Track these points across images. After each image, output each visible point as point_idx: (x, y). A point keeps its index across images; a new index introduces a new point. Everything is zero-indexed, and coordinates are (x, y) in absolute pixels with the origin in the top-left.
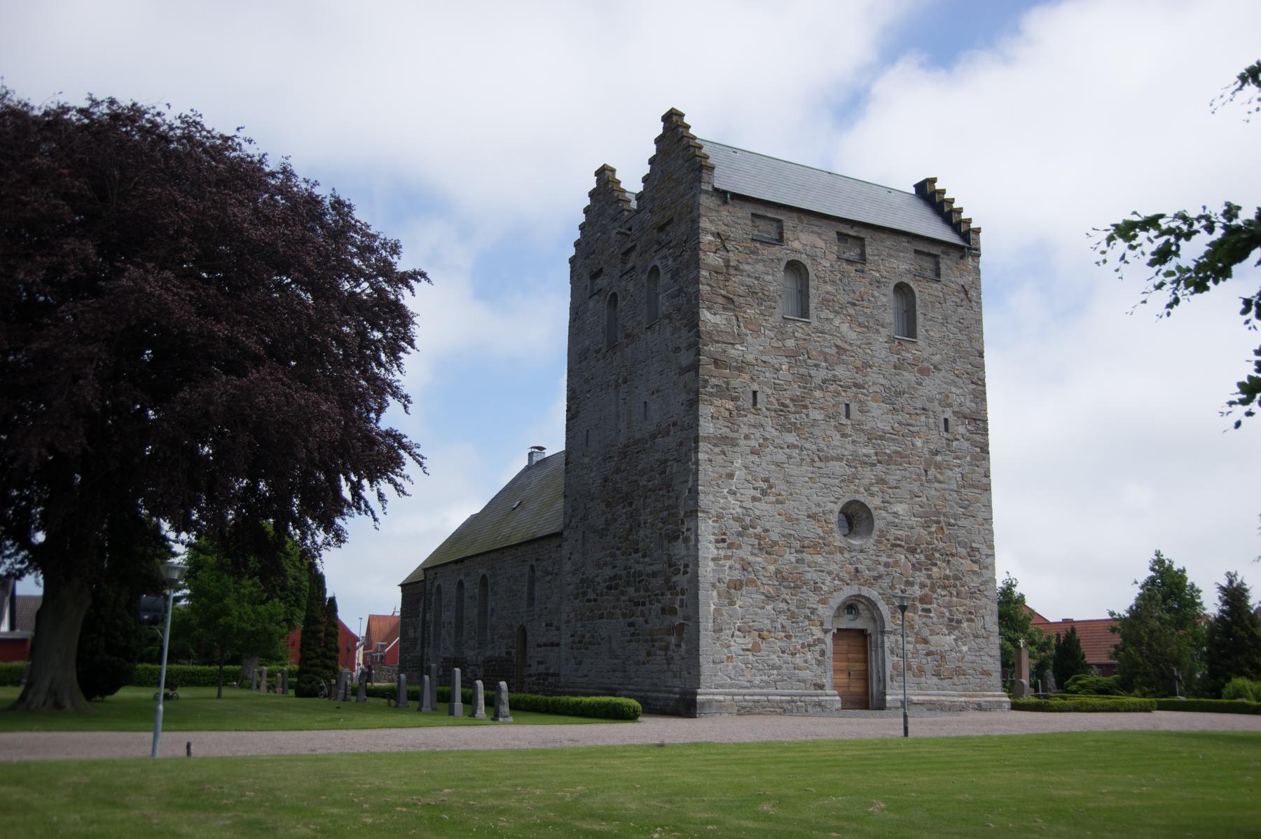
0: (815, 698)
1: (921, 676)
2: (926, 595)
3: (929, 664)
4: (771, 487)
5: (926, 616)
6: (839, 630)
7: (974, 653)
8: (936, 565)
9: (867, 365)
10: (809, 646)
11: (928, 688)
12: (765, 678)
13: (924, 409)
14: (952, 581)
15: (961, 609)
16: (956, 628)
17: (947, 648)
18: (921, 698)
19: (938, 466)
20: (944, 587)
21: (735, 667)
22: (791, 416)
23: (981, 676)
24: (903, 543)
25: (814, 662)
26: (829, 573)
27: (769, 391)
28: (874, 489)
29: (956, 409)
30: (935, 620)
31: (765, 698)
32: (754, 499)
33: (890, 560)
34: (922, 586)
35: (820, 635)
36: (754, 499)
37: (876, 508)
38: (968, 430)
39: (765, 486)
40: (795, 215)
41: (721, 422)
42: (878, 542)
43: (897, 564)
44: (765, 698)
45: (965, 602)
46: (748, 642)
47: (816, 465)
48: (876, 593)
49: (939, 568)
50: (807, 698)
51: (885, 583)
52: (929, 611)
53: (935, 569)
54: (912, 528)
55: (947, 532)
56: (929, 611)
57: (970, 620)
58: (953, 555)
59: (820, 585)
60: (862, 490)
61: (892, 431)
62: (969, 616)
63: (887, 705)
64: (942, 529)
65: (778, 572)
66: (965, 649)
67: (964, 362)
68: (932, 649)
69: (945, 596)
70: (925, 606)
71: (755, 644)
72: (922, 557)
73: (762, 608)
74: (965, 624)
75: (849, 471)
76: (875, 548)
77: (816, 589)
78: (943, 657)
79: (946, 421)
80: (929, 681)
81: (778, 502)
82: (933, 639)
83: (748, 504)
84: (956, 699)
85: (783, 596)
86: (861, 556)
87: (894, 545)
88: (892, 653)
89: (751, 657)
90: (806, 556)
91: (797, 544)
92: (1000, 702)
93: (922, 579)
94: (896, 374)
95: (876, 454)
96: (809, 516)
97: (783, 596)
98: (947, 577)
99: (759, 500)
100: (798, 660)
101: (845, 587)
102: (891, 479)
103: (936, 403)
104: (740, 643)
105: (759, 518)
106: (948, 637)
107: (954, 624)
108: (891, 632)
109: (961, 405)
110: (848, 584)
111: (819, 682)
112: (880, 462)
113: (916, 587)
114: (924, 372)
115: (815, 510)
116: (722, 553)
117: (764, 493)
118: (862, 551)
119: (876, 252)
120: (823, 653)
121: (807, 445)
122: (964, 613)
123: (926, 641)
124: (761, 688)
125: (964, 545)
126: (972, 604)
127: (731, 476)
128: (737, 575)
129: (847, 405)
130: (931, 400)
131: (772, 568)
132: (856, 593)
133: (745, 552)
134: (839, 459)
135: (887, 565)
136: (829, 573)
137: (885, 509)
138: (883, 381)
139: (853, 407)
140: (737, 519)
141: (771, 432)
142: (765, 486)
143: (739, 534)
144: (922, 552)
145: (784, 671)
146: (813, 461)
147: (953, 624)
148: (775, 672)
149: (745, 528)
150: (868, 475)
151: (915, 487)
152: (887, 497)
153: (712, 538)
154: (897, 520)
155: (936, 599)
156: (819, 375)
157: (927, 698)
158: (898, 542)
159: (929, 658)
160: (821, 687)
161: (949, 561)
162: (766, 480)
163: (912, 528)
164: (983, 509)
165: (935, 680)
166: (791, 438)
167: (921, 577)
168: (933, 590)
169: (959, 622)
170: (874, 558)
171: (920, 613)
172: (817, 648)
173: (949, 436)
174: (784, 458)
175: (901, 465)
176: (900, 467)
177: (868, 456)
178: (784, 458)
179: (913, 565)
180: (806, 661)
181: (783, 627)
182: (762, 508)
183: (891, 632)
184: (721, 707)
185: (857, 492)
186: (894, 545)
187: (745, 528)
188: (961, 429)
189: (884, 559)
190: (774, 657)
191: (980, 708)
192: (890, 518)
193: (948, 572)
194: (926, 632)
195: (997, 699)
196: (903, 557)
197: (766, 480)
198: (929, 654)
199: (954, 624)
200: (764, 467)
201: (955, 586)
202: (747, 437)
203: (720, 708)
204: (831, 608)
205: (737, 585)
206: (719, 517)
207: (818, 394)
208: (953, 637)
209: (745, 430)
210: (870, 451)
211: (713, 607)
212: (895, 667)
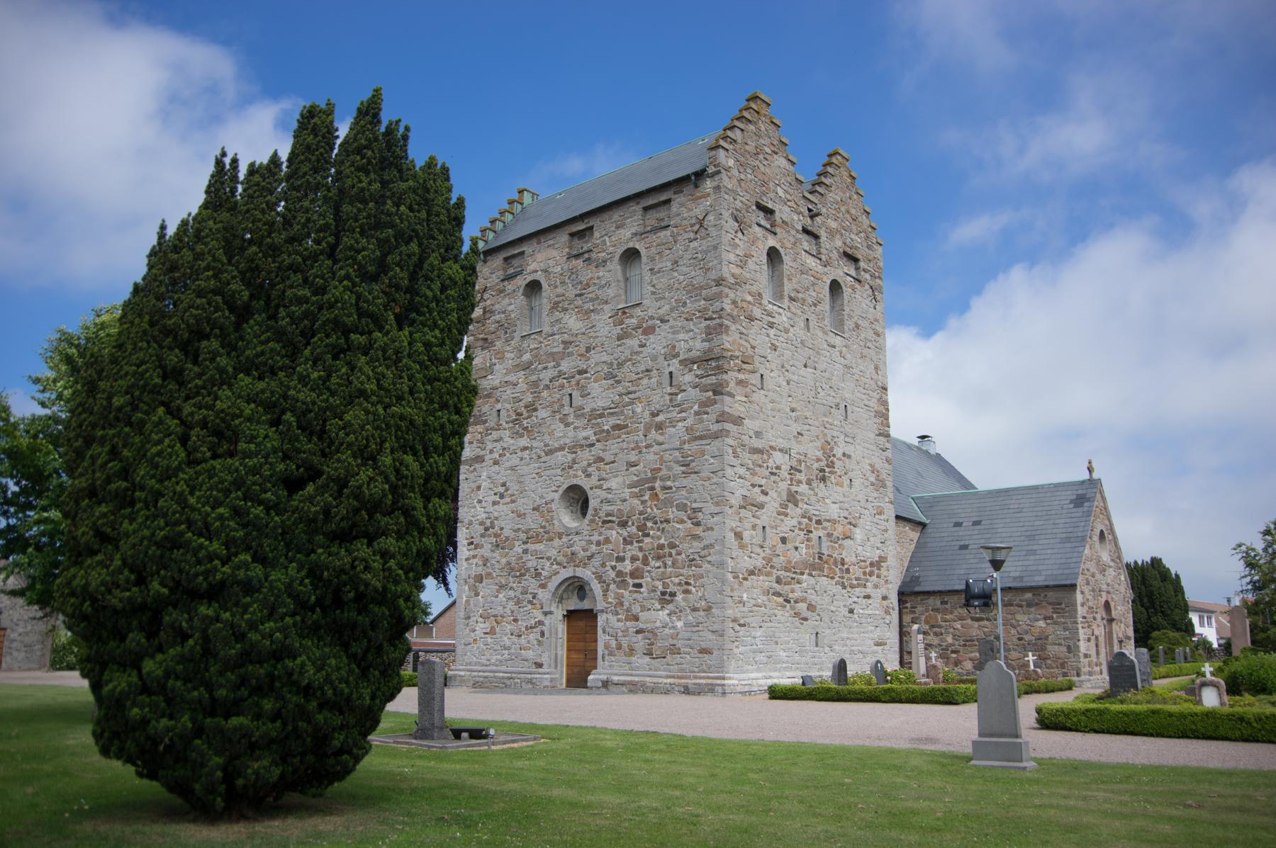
0: (529, 676)
1: (631, 655)
2: (637, 569)
3: (640, 642)
4: (507, 490)
5: (636, 592)
6: (568, 611)
7: (689, 629)
8: (648, 535)
9: (588, 349)
10: (531, 628)
11: (638, 668)
12: (499, 657)
13: (647, 371)
14: (667, 550)
15: (677, 580)
16: (672, 601)
17: (658, 624)
18: (622, 678)
19: (659, 427)
20: (658, 558)
21: (478, 648)
22: (525, 422)
23: (700, 655)
24: (614, 519)
25: (535, 642)
26: (549, 559)
27: (508, 406)
28: (590, 469)
29: (682, 357)
30: (645, 594)
31: (491, 674)
32: (494, 503)
33: (601, 538)
34: (634, 559)
35: (541, 617)
36: (494, 503)
37: (591, 488)
38: (697, 376)
39: (502, 490)
40: (535, 241)
41: (475, 444)
42: (592, 521)
43: (607, 541)
44: (491, 674)
45: (684, 571)
46: (486, 626)
47: (541, 460)
48: (590, 573)
49: (653, 538)
50: (523, 676)
51: (596, 562)
52: (640, 586)
53: (647, 540)
54: (625, 500)
55: (662, 497)
56: (640, 586)
57: (687, 592)
58: (667, 521)
59: (540, 571)
60: (580, 473)
61: (613, 406)
62: (686, 587)
63: (589, 684)
64: (656, 495)
65: (509, 563)
66: (679, 624)
67: (696, 301)
68: (641, 626)
69: (659, 567)
70: (637, 581)
71: (493, 628)
72: (634, 529)
73: (497, 597)
74: (679, 597)
75: (570, 457)
76: (589, 528)
77: (538, 575)
78: (655, 635)
79: (671, 373)
80: (640, 661)
81: (513, 502)
82: (643, 616)
83: (490, 509)
84: (660, 680)
85: (510, 585)
86: (576, 538)
87: (604, 522)
88: (604, 632)
89: (489, 640)
90: (531, 547)
91: (523, 536)
92: (712, 684)
93: (634, 553)
94: (619, 346)
95: (595, 434)
96: (534, 509)
97: (510, 585)
98: (661, 547)
99: (499, 503)
100: (523, 641)
101: (562, 571)
102: (608, 458)
103: (661, 359)
104: (482, 627)
105: (497, 519)
106: (660, 612)
107: (667, 597)
108: (602, 611)
109: (690, 350)
110: (564, 567)
111: (539, 661)
112: (598, 441)
113: (627, 562)
114: (650, 331)
115: (539, 502)
116: (472, 553)
117: (502, 496)
118: (577, 534)
119: (604, 233)
120: (543, 634)
121: (535, 444)
122: (680, 584)
123: (636, 619)
124: (497, 666)
125: (682, 507)
126: (691, 573)
127: (479, 488)
128: (480, 570)
129: (570, 395)
130: (654, 358)
131: (504, 561)
132: (571, 575)
133: (486, 551)
134: (561, 449)
135: (598, 543)
136: (549, 559)
137: (600, 487)
138: (605, 358)
139: (575, 394)
140: (482, 523)
141: (508, 441)
142: (502, 490)
143: (482, 536)
144: (633, 524)
145: (512, 651)
146: (539, 457)
147: (666, 597)
148: (507, 652)
149: (486, 529)
150: (585, 456)
151: (633, 457)
152: (604, 475)
153: (465, 542)
154: (610, 496)
155: (649, 572)
156: (546, 376)
157: (629, 678)
158: (610, 518)
159: (640, 636)
160: (540, 665)
161: (663, 529)
162: (504, 485)
163: (625, 500)
164: (712, 461)
165: (647, 659)
166: (524, 442)
167: (633, 550)
168: (645, 561)
169: (673, 594)
170: (587, 538)
171: (631, 588)
172: (538, 630)
173: (674, 390)
174: (517, 462)
175: (619, 437)
176: (621, 440)
177: (586, 438)
178: (517, 462)
179: (624, 539)
180: (529, 642)
181: (512, 612)
182: (502, 509)
183: (602, 611)
184: (461, 681)
185: (576, 476)
186: (604, 522)
187: (486, 529)
188: (688, 378)
189: (596, 538)
190: (505, 639)
191: (687, 691)
192: (603, 494)
193: (662, 541)
194: (636, 609)
195: (710, 681)
196: (614, 532)
197: (504, 485)
198: (638, 632)
199: (667, 597)
200: (502, 473)
201: (670, 555)
202: (491, 452)
203: (463, 681)
204: (550, 591)
205: (479, 579)
206: (470, 523)
207: (545, 394)
208: (667, 612)
209: (490, 446)
210: (589, 432)
211: (465, 599)
212: (607, 646)
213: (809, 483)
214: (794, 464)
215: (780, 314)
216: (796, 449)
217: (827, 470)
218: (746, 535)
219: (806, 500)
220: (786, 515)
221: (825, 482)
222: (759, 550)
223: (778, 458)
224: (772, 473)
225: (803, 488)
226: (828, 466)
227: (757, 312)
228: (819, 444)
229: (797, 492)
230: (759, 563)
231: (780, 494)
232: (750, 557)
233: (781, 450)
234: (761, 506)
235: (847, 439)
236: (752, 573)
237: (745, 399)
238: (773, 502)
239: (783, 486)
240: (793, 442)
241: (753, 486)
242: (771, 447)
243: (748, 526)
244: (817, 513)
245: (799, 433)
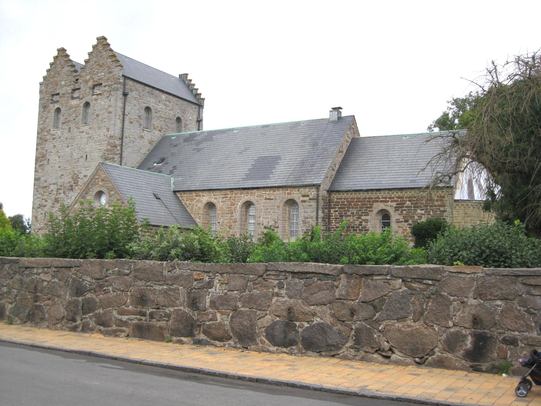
213: (64, 193)
214: (59, 187)
215: (58, 132)
216: (60, 181)
217: (74, 185)
218: (39, 217)
219: (62, 199)
220: (54, 207)
221: (72, 190)
222: (43, 221)
223: (52, 187)
224: (50, 193)
225: (62, 195)
226: (75, 183)
227: (48, 137)
228: (71, 176)
229: (58, 198)
230: (42, 225)
231: (52, 200)
232: (40, 224)
233: (54, 184)
234: (45, 206)
235: (86, 169)
236: (40, 229)
237: (41, 171)
238: (49, 203)
239: (53, 197)
240: (59, 179)
241: (43, 200)
242: (50, 184)
243: (39, 213)
244: (67, 203)
245: (61, 175)
